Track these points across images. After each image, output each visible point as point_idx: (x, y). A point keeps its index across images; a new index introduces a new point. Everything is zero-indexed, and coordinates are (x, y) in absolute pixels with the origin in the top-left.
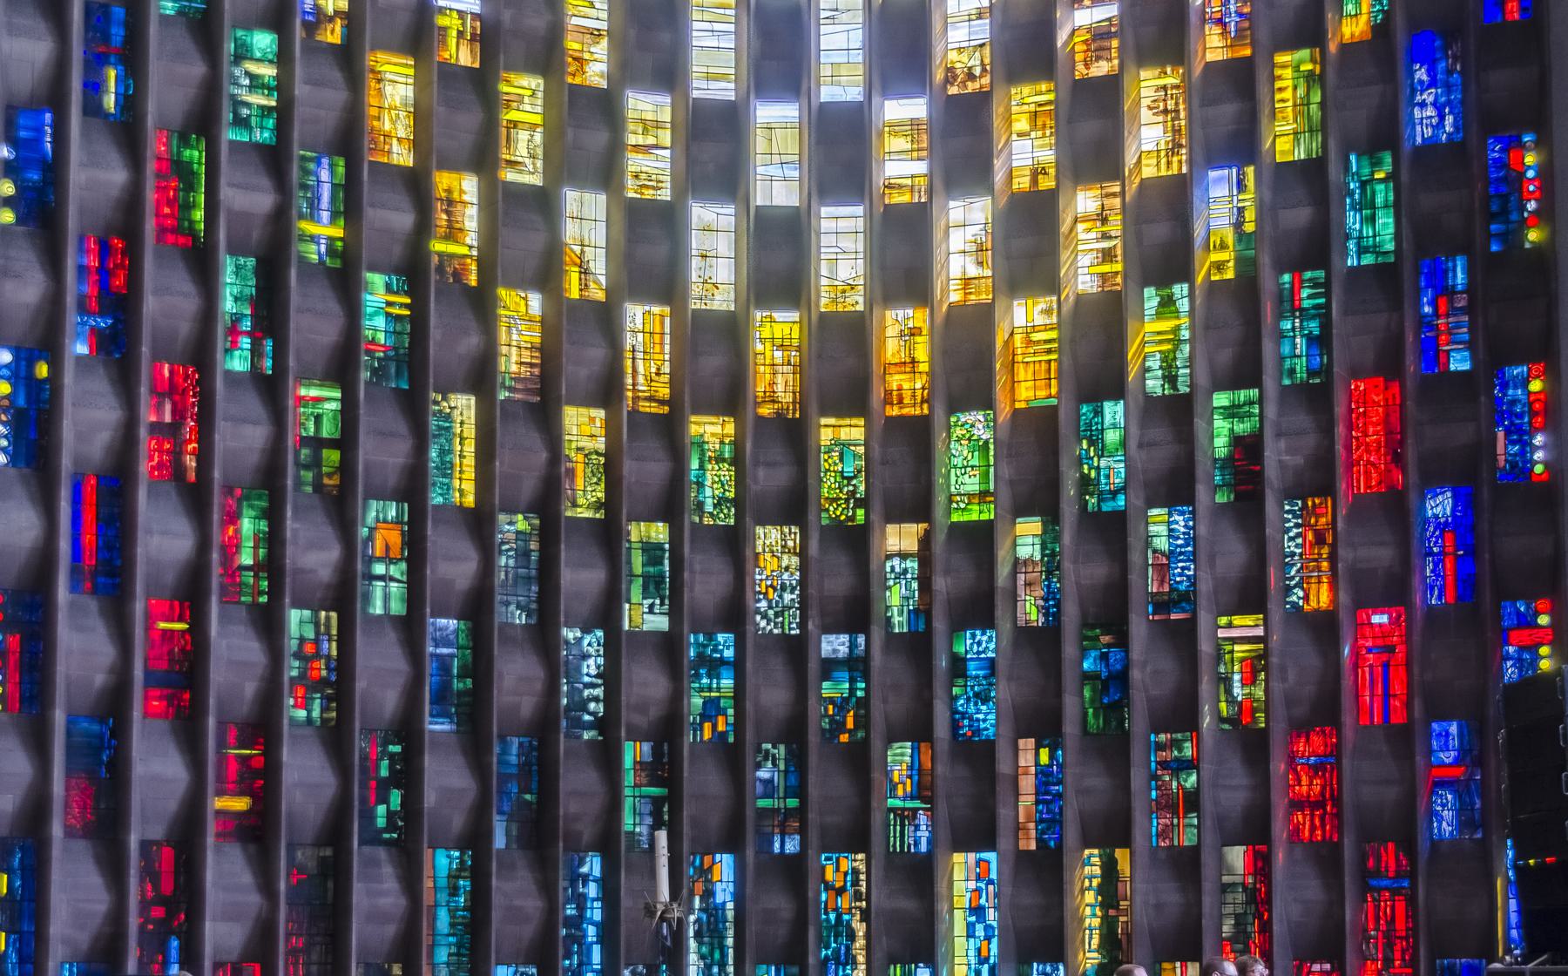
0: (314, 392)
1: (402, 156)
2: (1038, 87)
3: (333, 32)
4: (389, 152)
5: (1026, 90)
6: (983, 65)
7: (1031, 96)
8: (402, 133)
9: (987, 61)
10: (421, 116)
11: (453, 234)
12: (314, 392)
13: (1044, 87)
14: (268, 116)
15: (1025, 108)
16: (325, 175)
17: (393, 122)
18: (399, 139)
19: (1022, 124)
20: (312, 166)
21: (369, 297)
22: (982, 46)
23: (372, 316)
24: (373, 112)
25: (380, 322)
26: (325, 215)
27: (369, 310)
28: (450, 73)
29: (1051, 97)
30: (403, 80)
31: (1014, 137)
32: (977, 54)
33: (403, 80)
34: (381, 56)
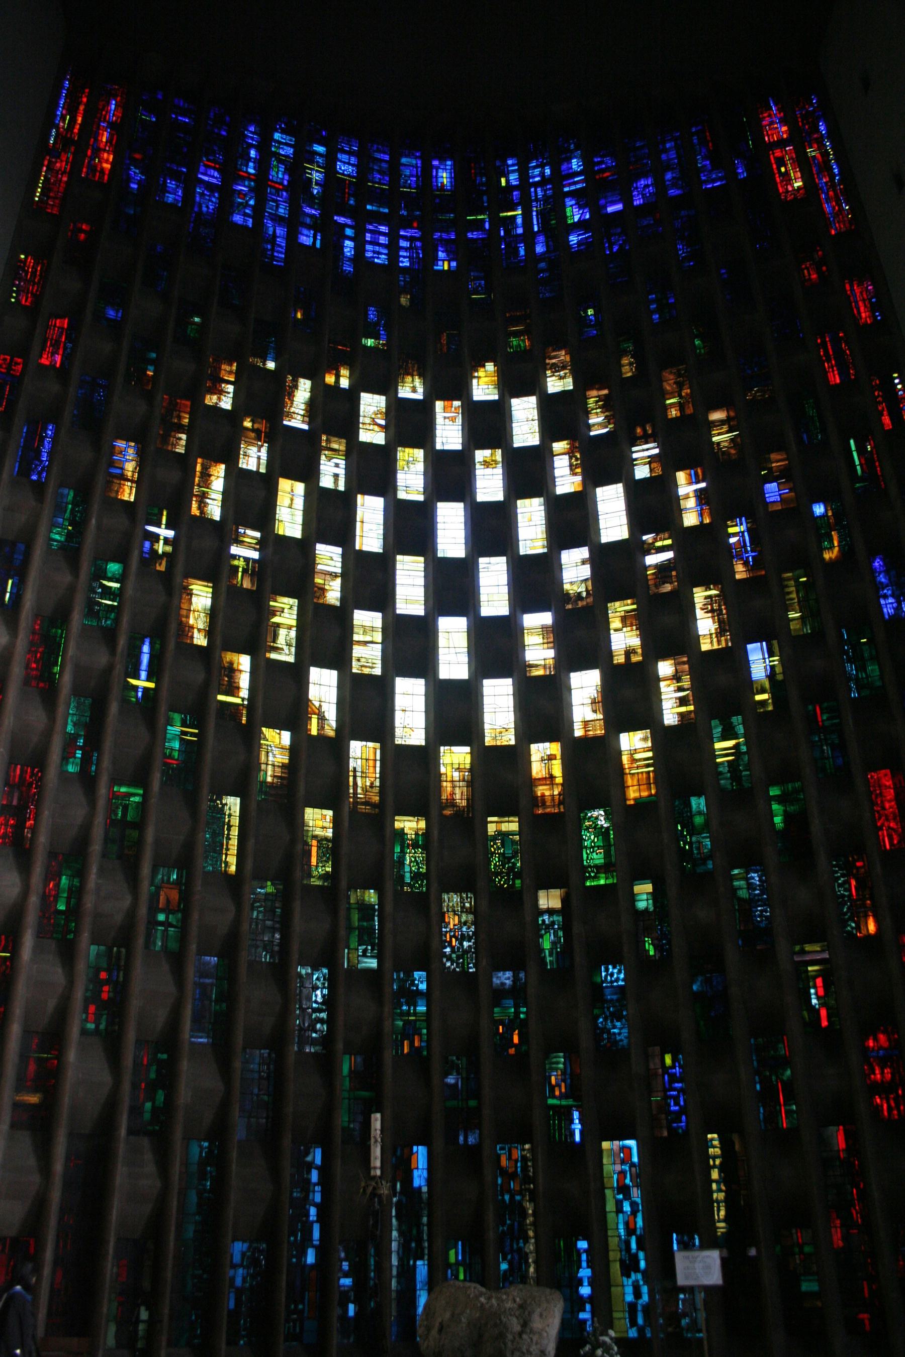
0: (123, 790)
1: (200, 640)
2: (625, 601)
3: (160, 564)
4: (192, 637)
5: (617, 604)
6: (587, 591)
7: (618, 609)
8: (201, 626)
9: (590, 588)
10: (213, 613)
11: (233, 689)
12: (123, 790)
13: (629, 601)
14: (112, 612)
15: (618, 614)
16: (146, 648)
17: (196, 619)
18: (199, 630)
19: (615, 623)
20: (138, 643)
21: (169, 728)
22: (586, 580)
23: (170, 741)
24: (184, 612)
25: (176, 745)
26: (143, 674)
27: (168, 736)
28: (237, 592)
29: (635, 607)
30: (205, 594)
31: (612, 632)
32: (583, 585)
33: (205, 594)
34: (191, 580)
